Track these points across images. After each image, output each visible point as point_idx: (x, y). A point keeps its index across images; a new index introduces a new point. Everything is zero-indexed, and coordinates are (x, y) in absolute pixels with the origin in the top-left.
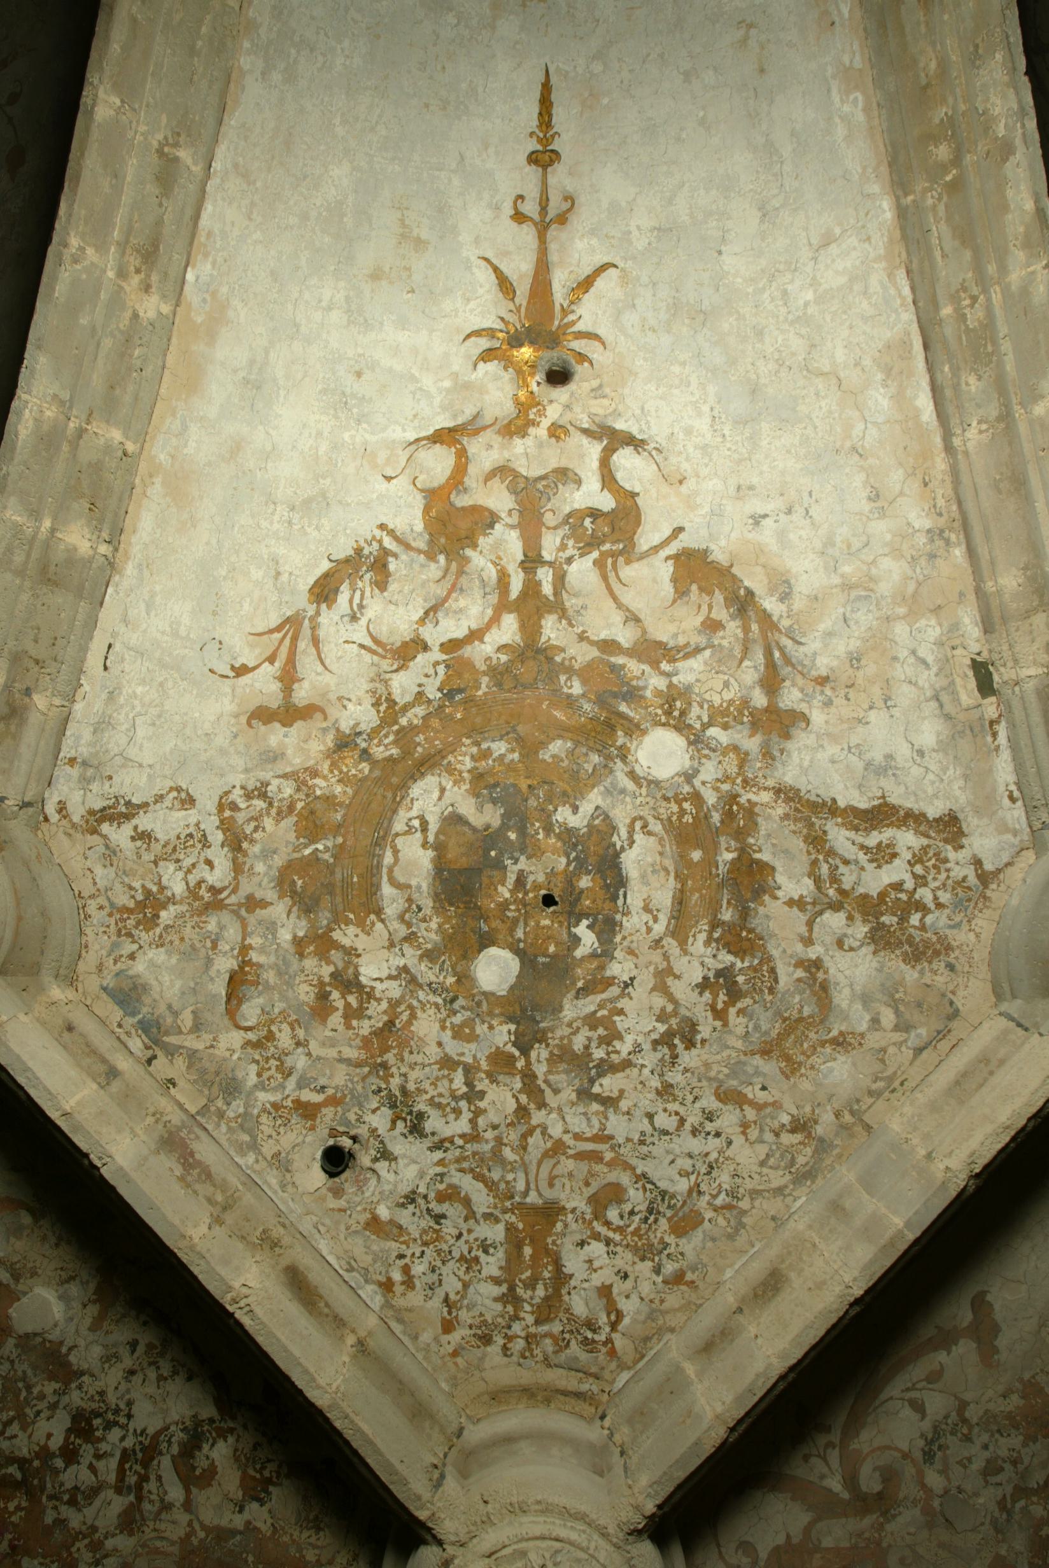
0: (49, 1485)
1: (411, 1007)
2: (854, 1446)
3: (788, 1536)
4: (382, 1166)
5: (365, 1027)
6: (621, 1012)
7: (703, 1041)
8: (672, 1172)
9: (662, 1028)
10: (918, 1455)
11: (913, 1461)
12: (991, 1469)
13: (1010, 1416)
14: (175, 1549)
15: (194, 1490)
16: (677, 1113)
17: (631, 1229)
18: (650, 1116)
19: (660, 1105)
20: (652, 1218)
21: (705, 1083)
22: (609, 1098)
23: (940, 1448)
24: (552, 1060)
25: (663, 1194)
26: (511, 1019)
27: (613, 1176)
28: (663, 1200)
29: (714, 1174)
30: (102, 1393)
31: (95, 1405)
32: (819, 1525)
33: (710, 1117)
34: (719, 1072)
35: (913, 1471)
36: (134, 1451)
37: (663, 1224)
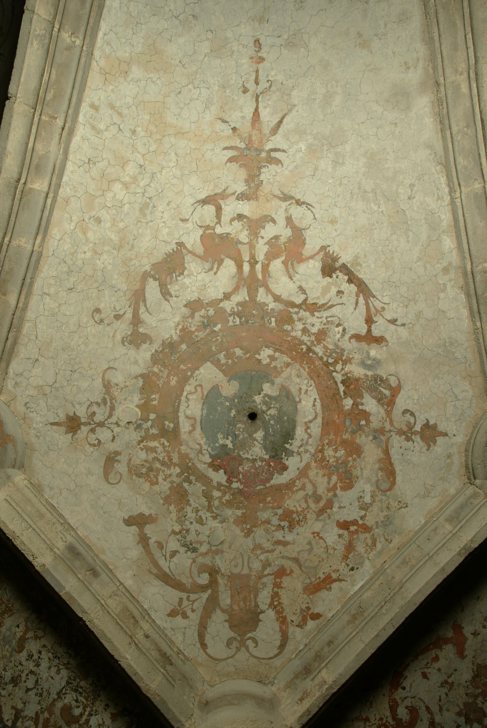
2: (189, 586)
3: (226, 621)
8: (57, 678)
10: (194, 555)
11: (196, 558)
12: (200, 521)
13: (179, 511)
16: (27, 675)
17: (84, 701)
18: (28, 690)
19: (22, 684)
20: (80, 690)
21: (13, 659)
22: (15, 715)
23: (191, 544)
25: (68, 683)
27: (57, 712)
28: (71, 683)
29: (59, 655)
32: (222, 605)
33: (30, 656)
34: (7, 651)
35: (200, 558)
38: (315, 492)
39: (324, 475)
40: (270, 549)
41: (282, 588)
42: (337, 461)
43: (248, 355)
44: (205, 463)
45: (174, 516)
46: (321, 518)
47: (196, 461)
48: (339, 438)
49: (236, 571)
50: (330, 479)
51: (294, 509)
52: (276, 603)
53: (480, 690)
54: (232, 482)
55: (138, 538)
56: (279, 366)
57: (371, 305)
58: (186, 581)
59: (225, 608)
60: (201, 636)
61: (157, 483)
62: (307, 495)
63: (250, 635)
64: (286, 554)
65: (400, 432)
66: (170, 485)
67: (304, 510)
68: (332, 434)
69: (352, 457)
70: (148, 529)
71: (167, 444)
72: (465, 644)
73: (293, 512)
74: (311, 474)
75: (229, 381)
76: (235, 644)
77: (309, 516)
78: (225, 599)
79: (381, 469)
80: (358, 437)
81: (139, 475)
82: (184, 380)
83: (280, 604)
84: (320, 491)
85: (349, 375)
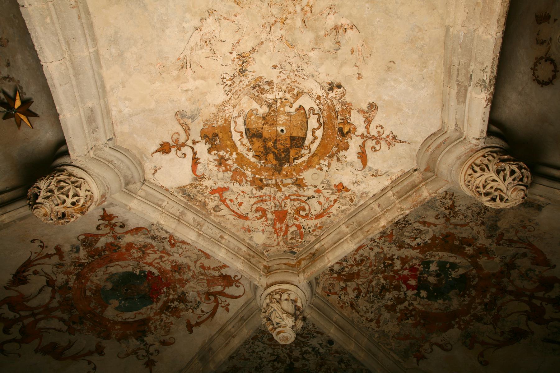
1: (316, 370)
2: (215, 304)
4: (321, 342)
5: (326, 366)
6: (271, 371)
7: (253, 368)
9: (262, 369)
13: (183, 311)
24: (286, 361)
26: (295, 368)
30: (378, 303)
31: (380, 300)
37: (259, 337)
38: (158, 258)
39: (149, 256)
42: (139, 252)
43: (93, 300)
45: (185, 313)
46: (171, 254)
47: (157, 309)
49: (206, 285)
50: (149, 253)
53: (244, 179)
54: (164, 292)
55: (197, 327)
56: (94, 286)
57: (36, 258)
58: (214, 304)
60: (236, 297)
61: (171, 322)
62: (161, 261)
63: (233, 279)
64: (194, 266)
65: (112, 229)
70: (193, 323)
71: (151, 322)
72: (221, 188)
73: (172, 266)
74: (149, 261)
75: (111, 304)
76: (238, 284)
78: (219, 288)
79: (137, 234)
81: (169, 330)
82: (116, 323)
83: (217, 267)
84: (158, 257)
85: (87, 256)
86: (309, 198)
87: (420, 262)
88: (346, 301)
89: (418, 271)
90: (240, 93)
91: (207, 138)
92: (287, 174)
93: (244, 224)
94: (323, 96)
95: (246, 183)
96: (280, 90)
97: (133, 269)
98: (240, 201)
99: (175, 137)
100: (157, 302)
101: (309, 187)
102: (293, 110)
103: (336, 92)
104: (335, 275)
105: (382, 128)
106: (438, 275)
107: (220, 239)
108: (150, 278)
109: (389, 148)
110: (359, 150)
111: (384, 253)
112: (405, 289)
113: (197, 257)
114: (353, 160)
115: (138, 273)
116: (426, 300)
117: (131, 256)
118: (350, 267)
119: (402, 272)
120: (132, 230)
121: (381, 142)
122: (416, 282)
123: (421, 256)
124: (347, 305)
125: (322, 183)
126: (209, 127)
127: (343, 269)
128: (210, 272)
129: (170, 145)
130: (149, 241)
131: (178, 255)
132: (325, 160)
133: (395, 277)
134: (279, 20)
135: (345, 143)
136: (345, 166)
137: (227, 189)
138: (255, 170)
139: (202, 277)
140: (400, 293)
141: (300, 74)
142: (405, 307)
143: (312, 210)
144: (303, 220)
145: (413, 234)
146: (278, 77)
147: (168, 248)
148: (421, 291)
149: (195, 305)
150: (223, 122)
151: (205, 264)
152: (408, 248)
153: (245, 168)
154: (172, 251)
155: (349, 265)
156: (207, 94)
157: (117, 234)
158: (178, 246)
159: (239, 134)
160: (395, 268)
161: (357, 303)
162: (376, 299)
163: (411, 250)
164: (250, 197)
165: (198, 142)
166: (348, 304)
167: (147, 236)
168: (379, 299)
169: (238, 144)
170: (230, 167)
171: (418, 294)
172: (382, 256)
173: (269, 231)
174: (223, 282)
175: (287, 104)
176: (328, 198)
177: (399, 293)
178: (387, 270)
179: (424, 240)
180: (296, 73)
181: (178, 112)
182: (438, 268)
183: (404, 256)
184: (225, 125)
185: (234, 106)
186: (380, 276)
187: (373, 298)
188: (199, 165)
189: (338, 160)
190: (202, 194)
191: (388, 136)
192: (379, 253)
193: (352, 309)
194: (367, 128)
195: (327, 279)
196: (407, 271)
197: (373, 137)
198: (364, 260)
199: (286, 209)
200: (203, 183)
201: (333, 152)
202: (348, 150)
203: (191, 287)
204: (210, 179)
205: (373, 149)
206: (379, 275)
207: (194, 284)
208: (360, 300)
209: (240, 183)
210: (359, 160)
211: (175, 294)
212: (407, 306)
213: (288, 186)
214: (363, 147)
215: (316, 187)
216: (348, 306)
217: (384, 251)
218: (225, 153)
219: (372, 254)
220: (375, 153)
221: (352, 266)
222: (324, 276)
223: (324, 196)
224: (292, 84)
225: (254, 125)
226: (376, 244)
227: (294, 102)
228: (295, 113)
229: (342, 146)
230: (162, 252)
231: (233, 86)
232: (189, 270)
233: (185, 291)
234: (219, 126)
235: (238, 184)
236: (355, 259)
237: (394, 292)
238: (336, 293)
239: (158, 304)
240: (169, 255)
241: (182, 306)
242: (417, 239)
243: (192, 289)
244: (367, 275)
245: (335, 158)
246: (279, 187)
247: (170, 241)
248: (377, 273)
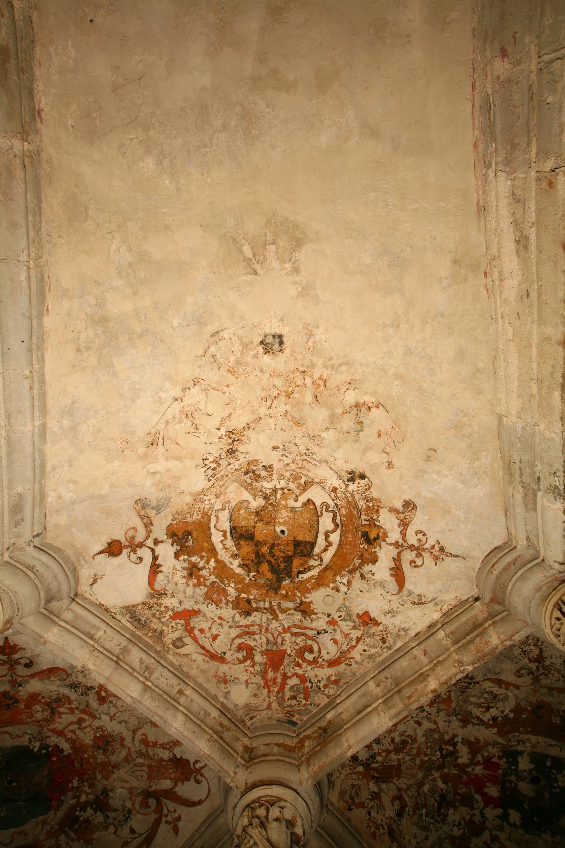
0: (452, 796)
2: (157, 816)
3: (183, 784)
10: (133, 812)
14: (403, 775)
15: (398, 794)
23: (125, 815)
31: (439, 825)
32: (171, 787)
35: (136, 806)
36: (422, 808)
38: (75, 723)
39: (60, 718)
40: (127, 750)
41: (156, 741)
44: (56, 814)
46: (98, 715)
48: (25, 711)
50: (62, 713)
51: (92, 736)
52: (168, 746)
53: (223, 599)
54: (73, 787)
58: (154, 816)
59: (173, 784)
60: (194, 804)
62: (79, 728)
63: (192, 766)
64: (130, 739)
65: (11, 668)
66: (75, 842)
67: (93, 729)
68: (21, 717)
69: (40, 700)
72: (188, 610)
73: (95, 737)
74: (60, 727)
76: (199, 777)
77: (98, 725)
78: (166, 784)
79: (49, 679)
80: (21, 697)
83: (168, 743)
84: (75, 719)
86: (318, 633)
87: (501, 751)
88: (379, 822)
89: (499, 769)
90: (226, 478)
91: (176, 538)
92: (287, 593)
93: (218, 670)
94: (341, 488)
95: (227, 604)
96: (282, 477)
97: (30, 741)
98: (214, 631)
99: (130, 533)
100: (57, 808)
101: (319, 615)
102: (298, 504)
103: (359, 483)
104: (360, 769)
105: (424, 535)
106: (534, 780)
107: (178, 695)
108: (54, 759)
109: (436, 564)
110: (393, 565)
111: (439, 732)
112: (482, 805)
113: (139, 723)
114: (385, 578)
115: (36, 750)
116: (520, 831)
117: (32, 716)
118: (384, 754)
119: (473, 769)
120: (43, 672)
121: (424, 554)
122: (498, 791)
123: (500, 740)
124: (382, 831)
125: (339, 610)
126: (180, 521)
127: (373, 757)
128: (155, 752)
129: (121, 544)
130: (65, 692)
131: (108, 718)
132: (343, 576)
133: (461, 777)
134: (284, 394)
135: (372, 553)
136: (373, 587)
137: (196, 613)
138: (240, 586)
139: (141, 760)
140: (474, 812)
141: (309, 459)
142: (485, 843)
143: (324, 653)
144: (309, 668)
145: (483, 700)
146: (280, 461)
147: (94, 704)
148: (510, 811)
149: (121, 818)
150: (200, 516)
151: (149, 736)
152: (478, 724)
153: (226, 582)
154: (100, 711)
155: (383, 751)
156: (181, 478)
157: (17, 678)
158: (111, 703)
159: (222, 533)
160: (460, 761)
161: (400, 827)
162: (432, 821)
163: (483, 728)
164: (231, 627)
165: (162, 542)
166: (384, 828)
167: (64, 682)
168: (437, 821)
169: (219, 547)
170: (205, 579)
171: (504, 817)
172: (437, 737)
173: (256, 684)
174: (175, 772)
175: (291, 496)
176: (348, 635)
177: (470, 812)
178: (447, 764)
179: (502, 712)
180: (304, 457)
181: (139, 500)
182: (532, 766)
183: (472, 739)
184: (202, 520)
185: (217, 496)
186: (436, 774)
187: (427, 819)
188: (160, 574)
189: (362, 577)
190: (159, 619)
191: (433, 547)
192: (431, 730)
193: (392, 842)
194: (403, 534)
195: (347, 775)
196: (481, 767)
197: (412, 547)
198: (408, 742)
199: (283, 648)
200: (163, 602)
201: (354, 565)
202: (377, 564)
203: (120, 779)
204: (174, 596)
205: (413, 564)
206: (434, 772)
207: (126, 773)
208: (404, 821)
209: (217, 604)
210: (393, 579)
211: (90, 793)
212: (489, 842)
213: (288, 612)
214: (397, 560)
215: (329, 615)
216: (384, 834)
217: (438, 727)
218: (199, 560)
219: (420, 732)
220: (416, 570)
221: (388, 752)
222: (342, 769)
223: (341, 631)
224: (298, 470)
225: (244, 523)
226: (425, 714)
227: (301, 494)
228: (301, 509)
229: (368, 557)
230: (83, 711)
231: (218, 470)
232: (123, 745)
233: (109, 788)
234: (194, 521)
235: (214, 606)
236: (393, 740)
237: (462, 808)
238: (362, 805)
239: (58, 813)
240: (94, 717)
241: (99, 818)
242: (490, 710)
243: (121, 784)
244: (414, 771)
245: (358, 574)
246: (275, 613)
247: (98, 693)
248: (430, 769)
